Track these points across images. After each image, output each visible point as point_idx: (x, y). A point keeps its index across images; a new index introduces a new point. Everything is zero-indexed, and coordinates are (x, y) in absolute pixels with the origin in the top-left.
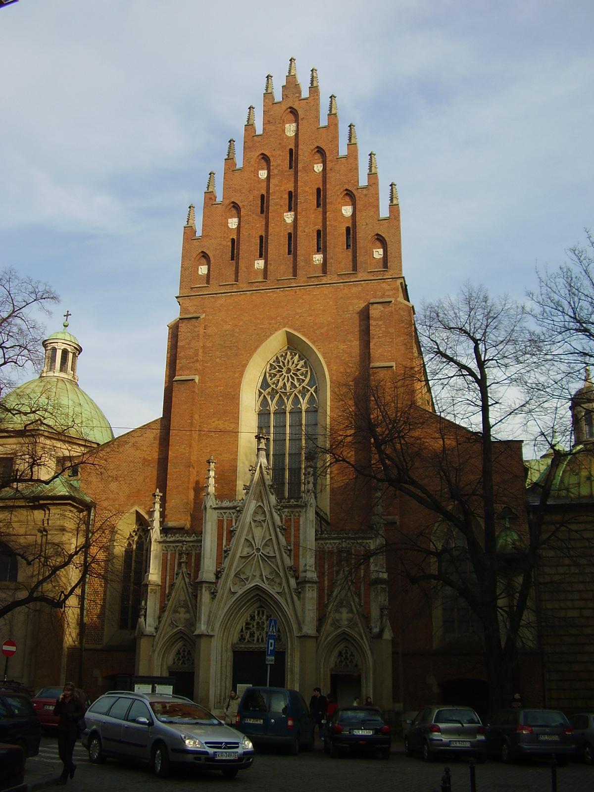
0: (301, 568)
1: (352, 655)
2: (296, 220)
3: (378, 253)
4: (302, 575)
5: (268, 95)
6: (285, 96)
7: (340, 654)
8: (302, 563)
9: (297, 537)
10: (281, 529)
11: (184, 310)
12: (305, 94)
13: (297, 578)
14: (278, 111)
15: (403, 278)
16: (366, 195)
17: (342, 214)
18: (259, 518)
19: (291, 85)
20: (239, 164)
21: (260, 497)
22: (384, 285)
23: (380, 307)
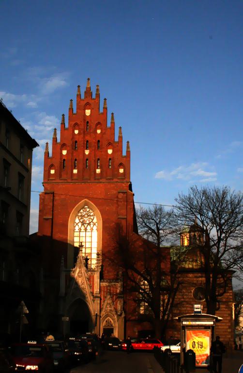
0: (95, 293)
1: (111, 322)
2: (89, 154)
3: (121, 171)
4: (95, 295)
5: (79, 96)
6: (86, 97)
7: (107, 321)
8: (95, 290)
9: (93, 281)
10: (88, 279)
11: (45, 189)
12: (94, 96)
13: (93, 296)
14: (83, 103)
15: (131, 182)
16: (117, 146)
17: (108, 153)
18: (80, 274)
19: (88, 92)
20: (67, 126)
21: (80, 268)
22: (124, 185)
23: (122, 194)
